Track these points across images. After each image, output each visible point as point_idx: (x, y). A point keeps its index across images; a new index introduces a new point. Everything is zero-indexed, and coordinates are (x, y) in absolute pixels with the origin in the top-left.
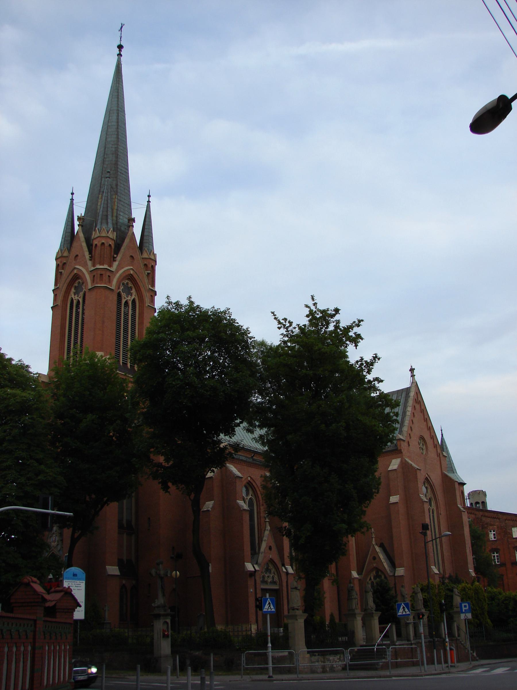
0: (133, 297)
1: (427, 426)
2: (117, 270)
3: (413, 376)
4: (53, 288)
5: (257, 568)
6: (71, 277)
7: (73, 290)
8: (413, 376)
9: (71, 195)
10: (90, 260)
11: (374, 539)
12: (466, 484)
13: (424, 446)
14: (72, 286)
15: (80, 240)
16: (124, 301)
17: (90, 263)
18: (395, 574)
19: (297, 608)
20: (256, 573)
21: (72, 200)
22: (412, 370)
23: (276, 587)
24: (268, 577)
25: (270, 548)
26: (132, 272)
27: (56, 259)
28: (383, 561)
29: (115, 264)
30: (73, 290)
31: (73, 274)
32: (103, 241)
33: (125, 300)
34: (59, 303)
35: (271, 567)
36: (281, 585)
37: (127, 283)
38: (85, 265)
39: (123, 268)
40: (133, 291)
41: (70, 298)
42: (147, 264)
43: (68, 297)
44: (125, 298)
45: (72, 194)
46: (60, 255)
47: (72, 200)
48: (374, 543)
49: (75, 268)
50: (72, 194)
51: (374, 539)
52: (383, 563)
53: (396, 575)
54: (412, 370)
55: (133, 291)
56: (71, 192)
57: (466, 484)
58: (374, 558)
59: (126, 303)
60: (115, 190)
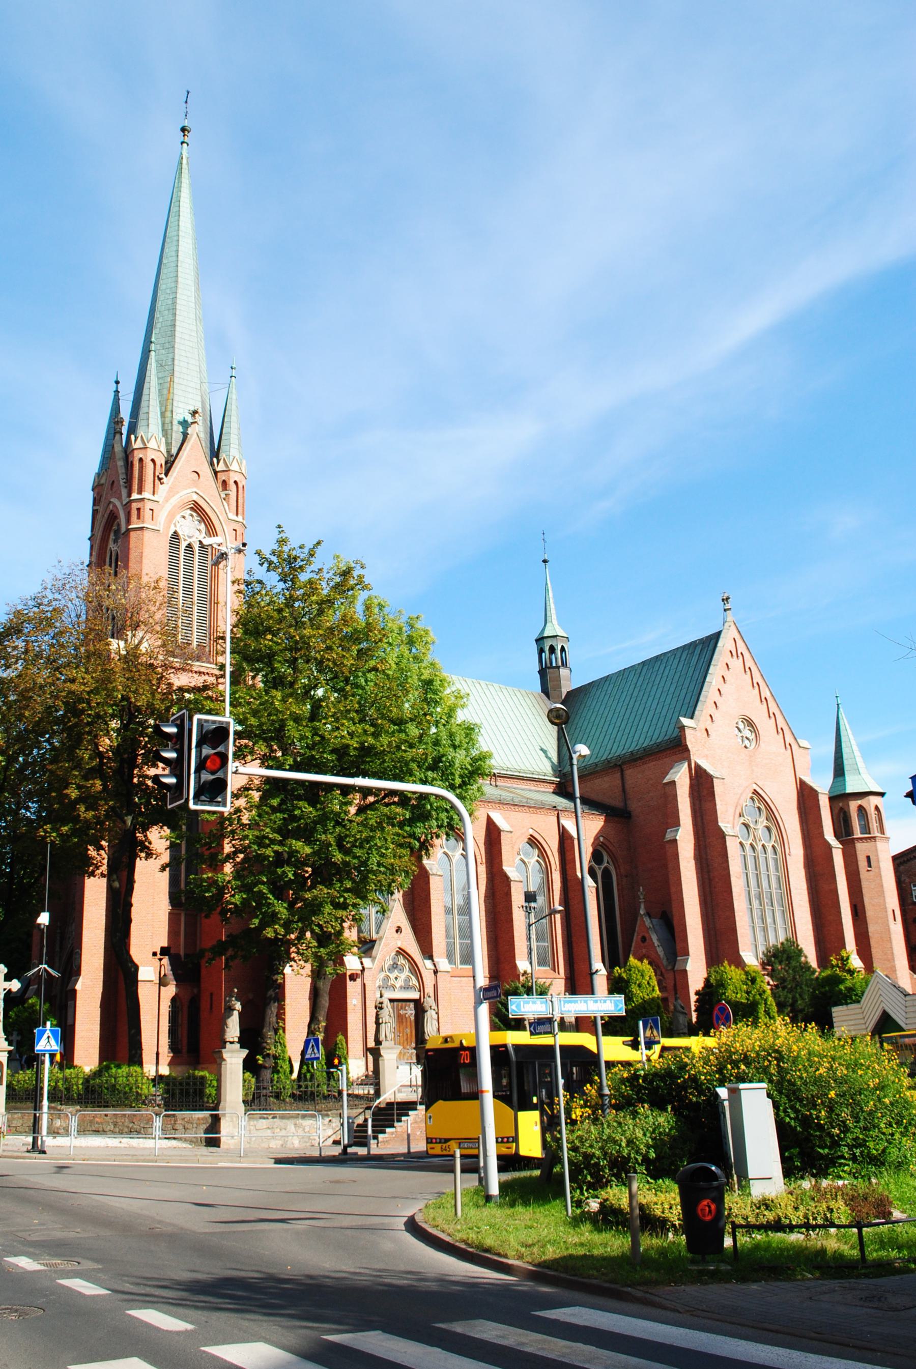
2: (167, 500)
4: (89, 535)
6: (106, 516)
7: (112, 536)
9: (115, 385)
10: (126, 487)
11: (642, 906)
12: (905, 796)
14: (110, 531)
15: (115, 458)
16: (183, 545)
17: (124, 492)
18: (674, 967)
19: (231, 1040)
20: (366, 973)
21: (117, 392)
23: (415, 995)
24: (396, 978)
26: (195, 497)
27: (93, 490)
28: (656, 943)
29: (162, 489)
30: (112, 536)
31: (108, 512)
32: (141, 456)
33: (186, 544)
34: (93, 559)
35: (402, 961)
36: (421, 988)
38: (120, 498)
39: (178, 492)
41: (108, 549)
42: (227, 480)
43: (106, 549)
44: (185, 540)
45: (117, 382)
46: (96, 484)
47: (117, 392)
48: (642, 912)
49: (110, 502)
50: (117, 382)
51: (642, 906)
52: (655, 947)
53: (676, 969)
56: (115, 379)
57: (905, 796)
58: (644, 939)
59: (189, 546)
60: (171, 368)
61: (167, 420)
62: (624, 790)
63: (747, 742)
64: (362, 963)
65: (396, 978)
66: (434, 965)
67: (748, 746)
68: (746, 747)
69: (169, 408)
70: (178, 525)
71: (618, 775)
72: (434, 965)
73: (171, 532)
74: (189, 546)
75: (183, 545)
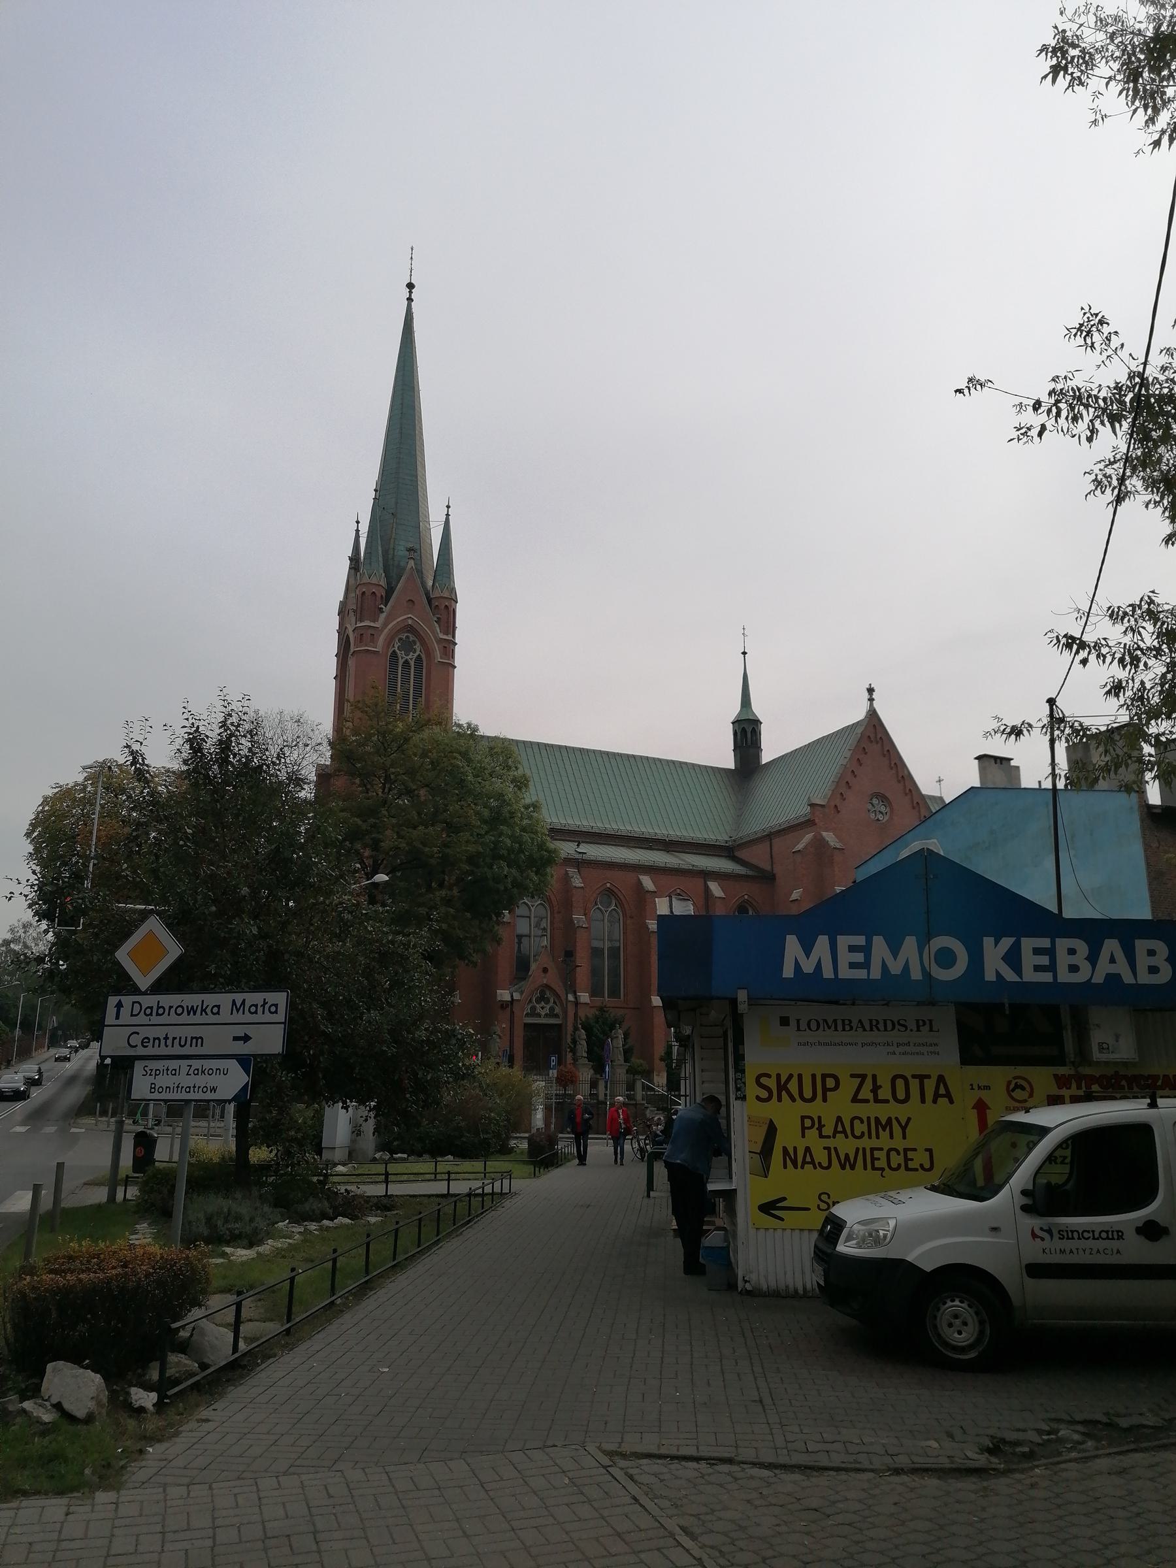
0: (416, 655)
1: (898, 777)
2: (385, 625)
3: (871, 700)
5: (516, 996)
8: (871, 700)
13: (888, 809)
16: (401, 662)
21: (357, 531)
22: (871, 691)
25: (545, 970)
26: (410, 622)
33: (404, 660)
37: (407, 637)
40: (418, 646)
54: (871, 691)
55: (418, 646)
59: (406, 663)
61: (390, 556)
62: (772, 856)
63: (880, 817)
64: (512, 996)
65: (543, 1008)
66: (576, 998)
67: (881, 819)
68: (878, 820)
69: (392, 546)
70: (396, 646)
71: (768, 843)
72: (576, 998)
73: (390, 651)
74: (406, 663)
75: (401, 662)
